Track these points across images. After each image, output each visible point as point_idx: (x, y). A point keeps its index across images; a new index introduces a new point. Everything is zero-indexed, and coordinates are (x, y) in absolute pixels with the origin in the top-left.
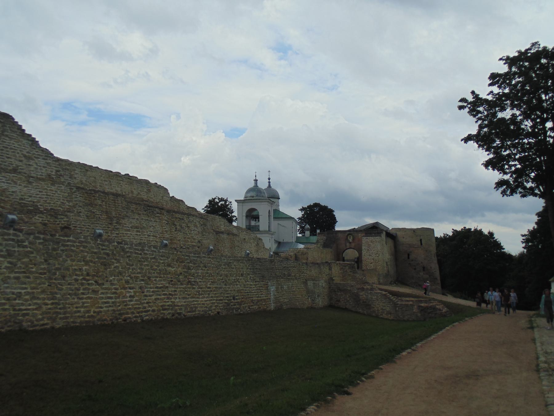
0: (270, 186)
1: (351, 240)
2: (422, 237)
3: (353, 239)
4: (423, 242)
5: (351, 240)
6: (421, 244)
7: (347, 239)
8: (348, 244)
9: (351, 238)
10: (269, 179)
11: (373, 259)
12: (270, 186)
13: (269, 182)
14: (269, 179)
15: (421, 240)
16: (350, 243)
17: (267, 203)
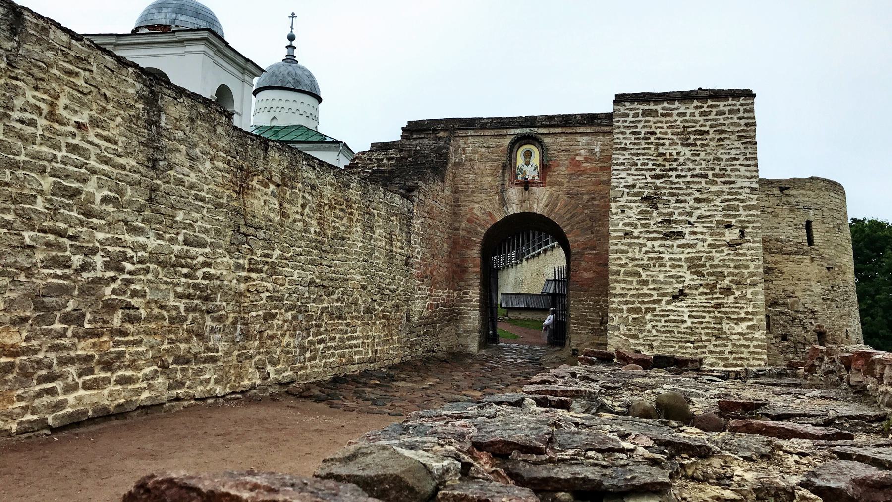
0: (291, 59)
1: (531, 172)
2: (811, 215)
3: (545, 168)
4: (816, 236)
5: (531, 172)
6: (810, 241)
7: (508, 165)
8: (514, 193)
9: (536, 160)
10: (291, 38)
11: (695, 266)
12: (291, 59)
13: (291, 47)
14: (291, 38)
15: (809, 224)
16: (526, 185)
17: (202, 48)
